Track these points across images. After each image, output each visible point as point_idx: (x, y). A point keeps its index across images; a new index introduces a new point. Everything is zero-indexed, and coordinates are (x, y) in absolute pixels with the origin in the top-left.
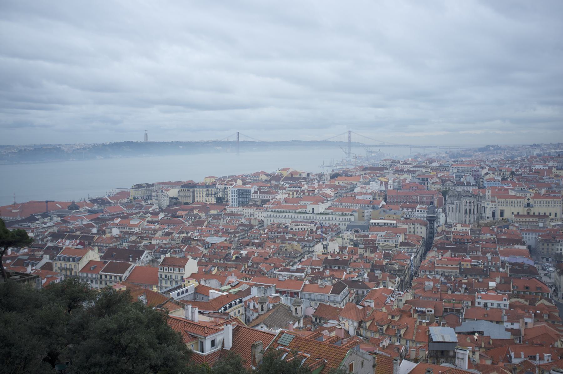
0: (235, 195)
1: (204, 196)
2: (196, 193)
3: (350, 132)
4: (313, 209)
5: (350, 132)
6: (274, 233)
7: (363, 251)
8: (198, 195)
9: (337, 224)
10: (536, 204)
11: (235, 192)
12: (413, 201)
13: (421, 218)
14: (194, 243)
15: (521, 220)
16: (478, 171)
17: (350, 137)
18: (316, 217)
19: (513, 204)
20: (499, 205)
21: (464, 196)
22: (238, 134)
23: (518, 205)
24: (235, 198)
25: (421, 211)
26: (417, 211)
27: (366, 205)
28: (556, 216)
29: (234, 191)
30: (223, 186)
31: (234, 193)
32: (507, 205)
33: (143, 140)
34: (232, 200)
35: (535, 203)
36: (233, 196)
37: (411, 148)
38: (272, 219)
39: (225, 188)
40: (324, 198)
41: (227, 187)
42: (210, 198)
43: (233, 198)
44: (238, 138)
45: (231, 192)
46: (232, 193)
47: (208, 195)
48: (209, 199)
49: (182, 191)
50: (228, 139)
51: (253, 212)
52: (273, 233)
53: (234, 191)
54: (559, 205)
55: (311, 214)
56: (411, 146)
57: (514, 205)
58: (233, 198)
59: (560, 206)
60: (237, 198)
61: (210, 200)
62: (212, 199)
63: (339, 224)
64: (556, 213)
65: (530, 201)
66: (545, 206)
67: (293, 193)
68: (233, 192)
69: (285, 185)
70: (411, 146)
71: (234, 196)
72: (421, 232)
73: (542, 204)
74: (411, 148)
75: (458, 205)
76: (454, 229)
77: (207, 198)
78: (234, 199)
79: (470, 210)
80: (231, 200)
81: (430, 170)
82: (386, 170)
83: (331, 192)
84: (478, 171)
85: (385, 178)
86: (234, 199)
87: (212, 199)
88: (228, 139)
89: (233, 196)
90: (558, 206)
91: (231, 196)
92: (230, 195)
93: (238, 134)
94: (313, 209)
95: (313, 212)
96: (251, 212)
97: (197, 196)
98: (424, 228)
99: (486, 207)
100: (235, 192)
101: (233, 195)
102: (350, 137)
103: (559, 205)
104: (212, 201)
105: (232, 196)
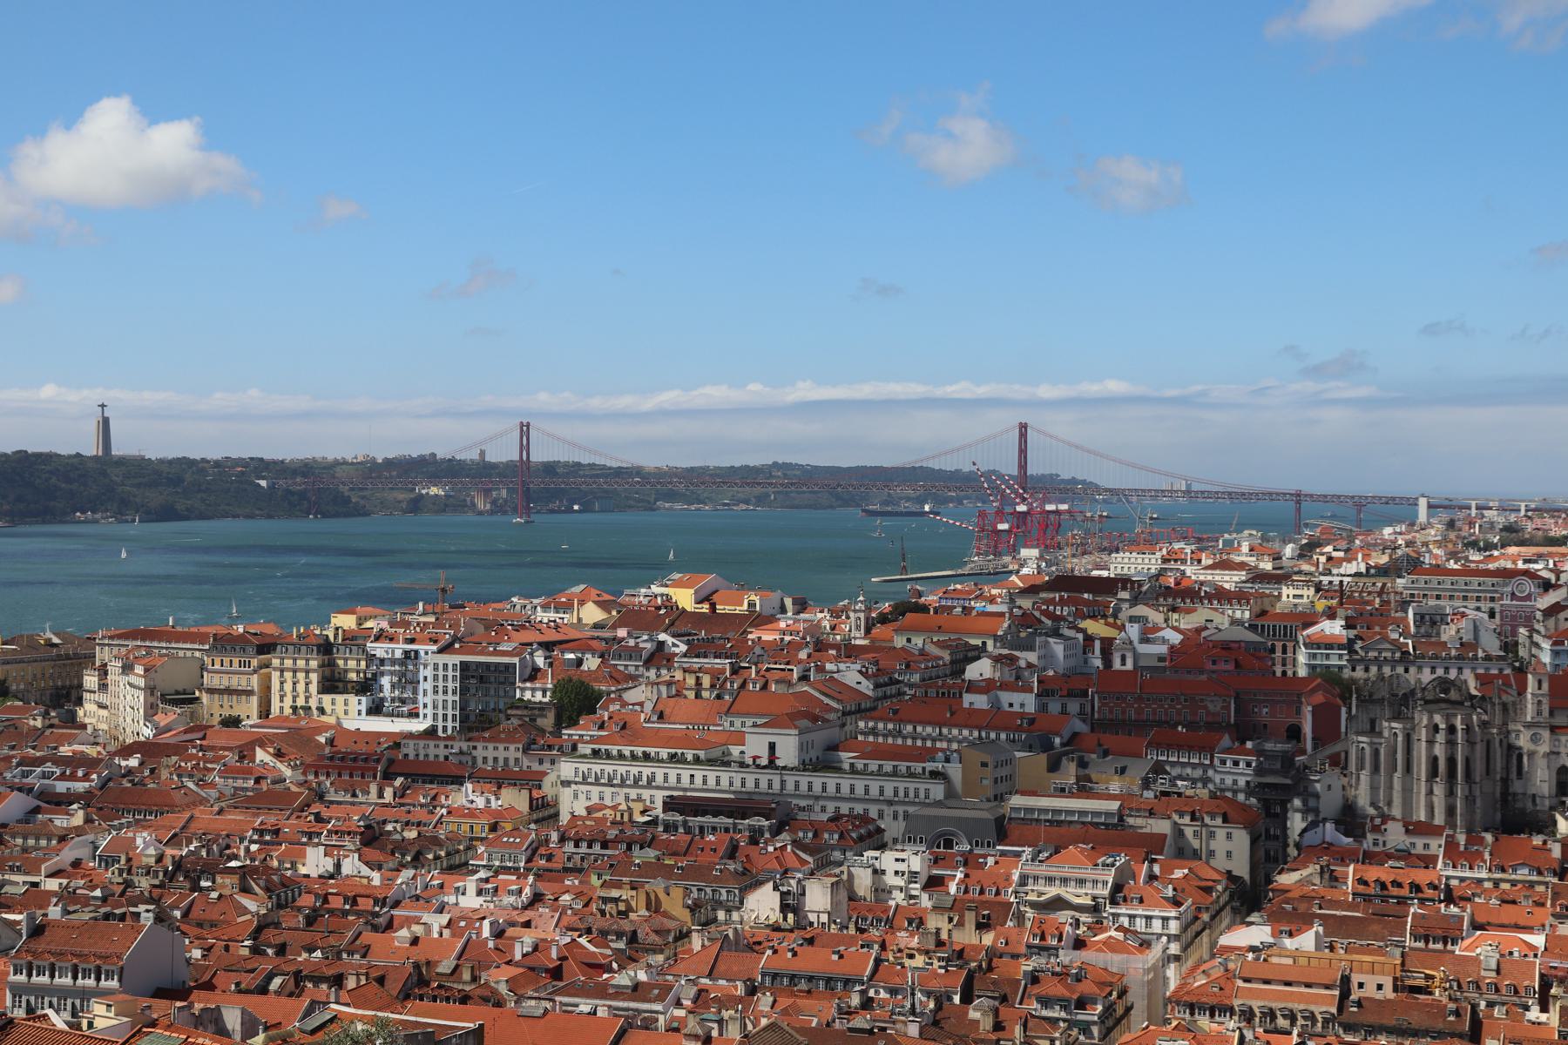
0: (450, 685)
1: (313, 688)
2: (275, 676)
3: (1023, 428)
4: (772, 746)
5: (1023, 428)
6: (590, 847)
7: (951, 920)
8: (288, 687)
9: (873, 814)
11: (450, 673)
12: (1210, 719)
13: (1235, 792)
14: (228, 881)
16: (1528, 597)
17: (1023, 451)
18: (783, 782)
21: (1427, 702)
22: (525, 429)
24: (450, 698)
25: (1236, 763)
26: (1217, 762)
27: (1003, 736)
29: (445, 666)
30: (399, 649)
31: (445, 678)
33: (90, 448)
34: (435, 707)
36: (440, 690)
37: (1298, 502)
38: (595, 790)
39: (407, 653)
40: (826, 700)
41: (416, 652)
42: (340, 698)
43: (441, 697)
44: (525, 447)
45: (429, 672)
46: (436, 678)
47: (332, 683)
48: (333, 704)
49: (217, 666)
50: (482, 453)
51: (517, 760)
52: (585, 844)
53: (445, 666)
55: (765, 767)
56: (1299, 495)
58: (441, 697)
60: (457, 698)
61: (340, 708)
62: (346, 704)
63: (881, 815)
67: (698, 682)
68: (441, 673)
69: (674, 645)
71: (445, 692)
72: (1229, 854)
75: (1400, 739)
76: (1376, 844)
77: (327, 699)
78: (445, 701)
79: (1451, 762)
80: (430, 706)
81: (1312, 590)
82: (1124, 589)
83: (861, 679)
84: (1528, 597)
85: (1107, 624)
86: (445, 701)
87: (346, 704)
88: (482, 453)
89: (440, 690)
91: (430, 691)
92: (429, 686)
93: (525, 429)
94: (772, 746)
96: (506, 760)
97: (282, 689)
98: (1242, 838)
100: (450, 673)
101: (441, 684)
102: (1023, 451)
104: (346, 713)
105: (435, 692)
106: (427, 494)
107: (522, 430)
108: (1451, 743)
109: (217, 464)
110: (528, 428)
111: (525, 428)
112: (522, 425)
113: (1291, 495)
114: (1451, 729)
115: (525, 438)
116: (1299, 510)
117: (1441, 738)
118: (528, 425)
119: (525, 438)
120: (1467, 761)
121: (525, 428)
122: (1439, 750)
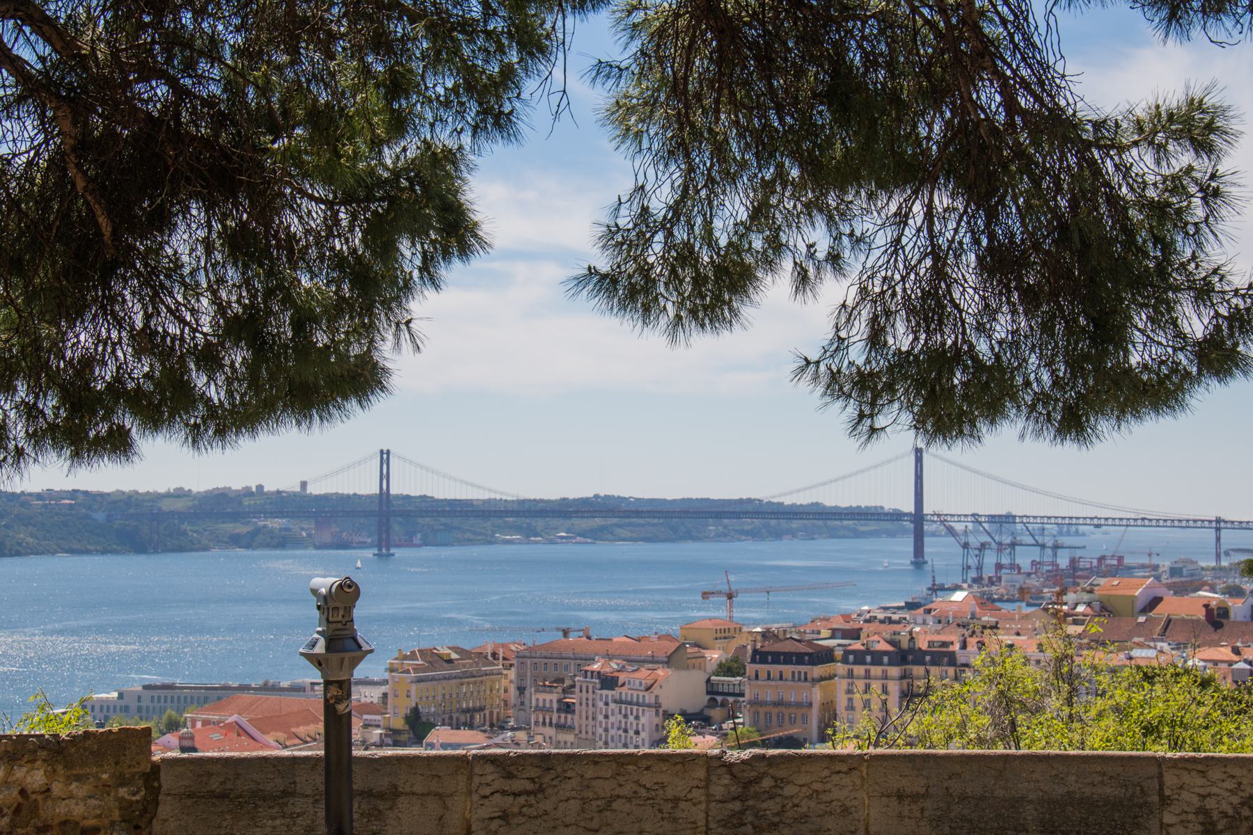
22: (385, 457)
37: (1218, 529)
44: (385, 476)
50: (304, 485)
56: (1218, 521)
70: (1219, 524)
74: (1218, 529)
88: (304, 485)
93: (385, 457)
107: (382, 458)
111: (385, 456)
112: (382, 452)
113: (1210, 522)
115: (385, 467)
116: (1218, 539)
118: (388, 452)
119: (385, 467)
121: (385, 456)
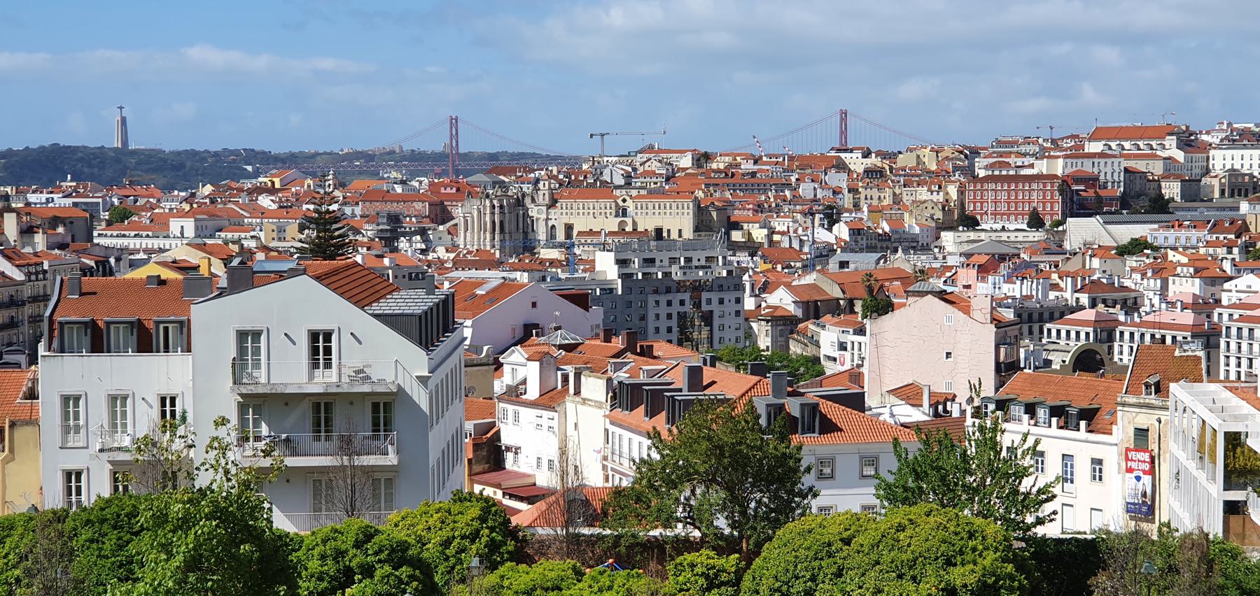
3: (844, 114)
5: (844, 114)
10: (639, 211)
15: (589, 241)
19: (591, 211)
20: (562, 214)
22: (454, 122)
23: (601, 213)
28: (680, 236)
32: (578, 214)
35: (636, 208)
44: (455, 136)
54: (686, 211)
57: (594, 213)
59: (688, 213)
64: (680, 231)
65: (626, 204)
66: (657, 214)
73: (650, 211)
79: (493, 223)
83: (271, 203)
90: (683, 213)
93: (454, 122)
95: (182, 233)
99: (537, 219)
103: (686, 211)
106: (389, 177)
108: (493, 213)
109: (216, 154)
110: (457, 122)
111: (454, 121)
114: (493, 207)
117: (497, 210)
118: (456, 120)
119: (454, 129)
120: (502, 223)
121: (454, 121)
122: (488, 219)
